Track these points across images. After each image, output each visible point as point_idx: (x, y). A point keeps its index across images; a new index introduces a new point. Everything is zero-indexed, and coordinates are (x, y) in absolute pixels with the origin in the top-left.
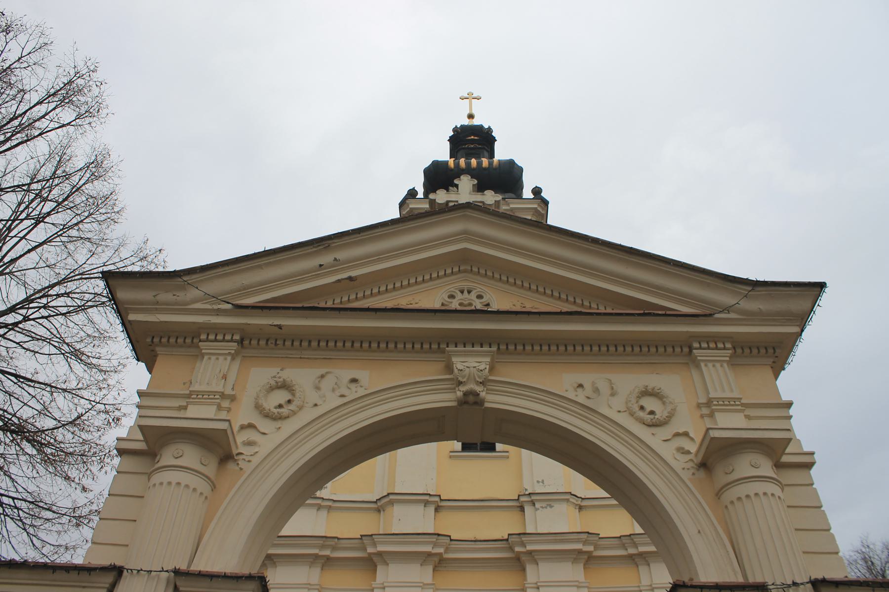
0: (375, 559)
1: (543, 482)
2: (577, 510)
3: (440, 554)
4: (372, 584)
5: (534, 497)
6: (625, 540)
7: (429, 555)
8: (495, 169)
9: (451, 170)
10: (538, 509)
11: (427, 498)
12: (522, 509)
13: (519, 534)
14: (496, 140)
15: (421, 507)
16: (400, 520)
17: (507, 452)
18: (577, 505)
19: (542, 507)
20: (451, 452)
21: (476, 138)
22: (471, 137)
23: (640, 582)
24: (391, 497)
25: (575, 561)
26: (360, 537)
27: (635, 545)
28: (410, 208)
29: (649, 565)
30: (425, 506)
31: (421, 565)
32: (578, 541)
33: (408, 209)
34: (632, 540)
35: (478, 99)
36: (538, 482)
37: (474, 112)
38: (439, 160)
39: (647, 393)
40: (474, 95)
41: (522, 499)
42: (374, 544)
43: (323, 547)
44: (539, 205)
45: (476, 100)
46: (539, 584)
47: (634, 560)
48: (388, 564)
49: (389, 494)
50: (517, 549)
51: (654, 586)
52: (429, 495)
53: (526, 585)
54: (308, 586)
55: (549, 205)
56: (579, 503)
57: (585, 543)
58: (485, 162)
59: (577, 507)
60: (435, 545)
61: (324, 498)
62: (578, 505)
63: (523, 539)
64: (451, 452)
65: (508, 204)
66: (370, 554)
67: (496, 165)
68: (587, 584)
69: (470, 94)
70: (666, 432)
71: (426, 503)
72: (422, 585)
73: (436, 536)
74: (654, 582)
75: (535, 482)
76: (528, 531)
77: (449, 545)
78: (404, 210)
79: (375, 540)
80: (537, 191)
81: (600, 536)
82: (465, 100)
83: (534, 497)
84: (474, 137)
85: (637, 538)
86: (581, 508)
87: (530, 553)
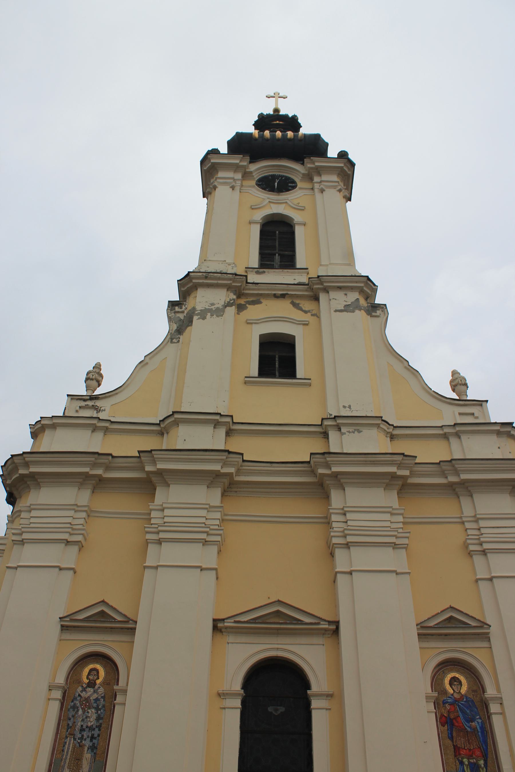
0: (154, 479)
1: (350, 407)
2: (389, 439)
3: (230, 475)
4: (149, 505)
6: (445, 467)
7: (217, 475)
8: (301, 140)
9: (256, 139)
10: (345, 434)
11: (217, 417)
13: (323, 454)
14: (301, 127)
16: (185, 440)
17: (310, 379)
18: (388, 433)
19: (349, 432)
20: (246, 377)
21: (281, 123)
22: (276, 121)
23: (462, 513)
24: (176, 416)
25: (387, 487)
26: (138, 455)
27: (457, 473)
28: (212, 163)
29: (471, 496)
30: (214, 428)
31: (208, 487)
32: (391, 463)
33: (210, 164)
34: (453, 466)
35: (284, 98)
36: (344, 407)
38: (243, 132)
40: (281, 95)
41: (326, 423)
42: (154, 462)
43: (94, 465)
44: (345, 165)
45: (282, 99)
46: (346, 509)
47: (454, 490)
48: (168, 486)
49: (174, 413)
50: (321, 471)
51: (478, 516)
52: (220, 414)
53: (331, 511)
54: (75, 507)
55: (356, 167)
56: (391, 430)
57: (400, 466)
58: (290, 134)
59: (389, 436)
60: (225, 464)
61: (101, 418)
62: (389, 432)
63: (328, 459)
64: (246, 377)
66: (148, 473)
67: (301, 137)
68: (402, 511)
71: (216, 424)
72: (207, 506)
73: (227, 453)
74: (477, 513)
75: (341, 407)
76: (332, 451)
77: (241, 466)
78: (205, 167)
79: (155, 456)
80: (343, 155)
81: (417, 461)
82: (271, 98)
83: (339, 421)
84: (279, 121)
85: (458, 464)
87: (336, 476)
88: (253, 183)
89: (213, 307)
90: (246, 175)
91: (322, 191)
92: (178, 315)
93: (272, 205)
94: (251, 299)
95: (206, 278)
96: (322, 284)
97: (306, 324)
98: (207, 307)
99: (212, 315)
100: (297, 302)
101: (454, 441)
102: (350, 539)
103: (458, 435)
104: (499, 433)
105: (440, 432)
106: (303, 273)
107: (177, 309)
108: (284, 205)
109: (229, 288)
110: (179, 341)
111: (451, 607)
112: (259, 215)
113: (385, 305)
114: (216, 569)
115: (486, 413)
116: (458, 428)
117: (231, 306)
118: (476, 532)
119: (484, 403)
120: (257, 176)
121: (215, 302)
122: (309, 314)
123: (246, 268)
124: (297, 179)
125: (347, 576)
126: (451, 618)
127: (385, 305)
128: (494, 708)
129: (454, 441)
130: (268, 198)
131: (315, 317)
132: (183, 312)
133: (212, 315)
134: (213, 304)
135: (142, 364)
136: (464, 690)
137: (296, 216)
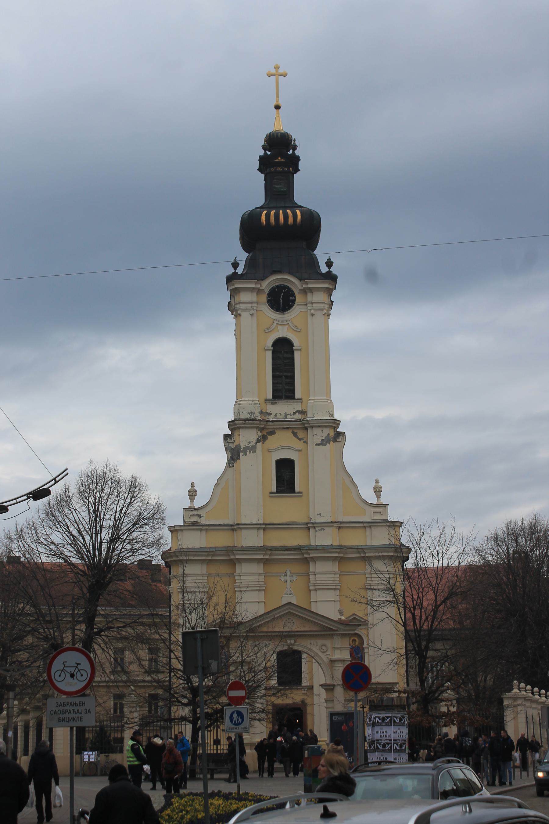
1: (320, 514)
5: (315, 525)
10: (317, 531)
12: (309, 528)
15: (256, 531)
17: (302, 493)
19: (319, 530)
36: (318, 514)
37: (281, 103)
39: (323, 645)
40: (281, 71)
43: (208, 555)
65: (307, 284)
69: (277, 68)
70: (325, 654)
71: (258, 529)
80: (329, 264)
82: (271, 76)
83: (315, 525)
86: (340, 528)
88: (264, 298)
89: (250, 445)
90: (259, 291)
91: (313, 315)
92: (230, 445)
93: (279, 326)
94: (269, 431)
95: (245, 424)
96: (309, 424)
97: (300, 451)
98: (247, 445)
99: (250, 452)
100: (295, 431)
101: (368, 529)
102: (317, 587)
103: (370, 527)
104: (389, 526)
105: (362, 525)
106: (299, 402)
107: (229, 440)
108: (287, 326)
109: (257, 428)
110: (233, 466)
111: (354, 614)
112: (270, 343)
113: (345, 432)
114: (264, 602)
115: (386, 513)
116: (370, 525)
117: (259, 443)
118: (370, 579)
119: (386, 506)
120: (267, 291)
121: (251, 441)
122: (302, 441)
123: (265, 400)
124: (296, 292)
125: (315, 603)
126: (354, 618)
127: (345, 432)
128: (366, 650)
129: (368, 529)
130: (276, 320)
131: (305, 444)
132: (233, 443)
133: (250, 452)
134: (249, 443)
135: (217, 485)
136: (357, 643)
137: (296, 343)
